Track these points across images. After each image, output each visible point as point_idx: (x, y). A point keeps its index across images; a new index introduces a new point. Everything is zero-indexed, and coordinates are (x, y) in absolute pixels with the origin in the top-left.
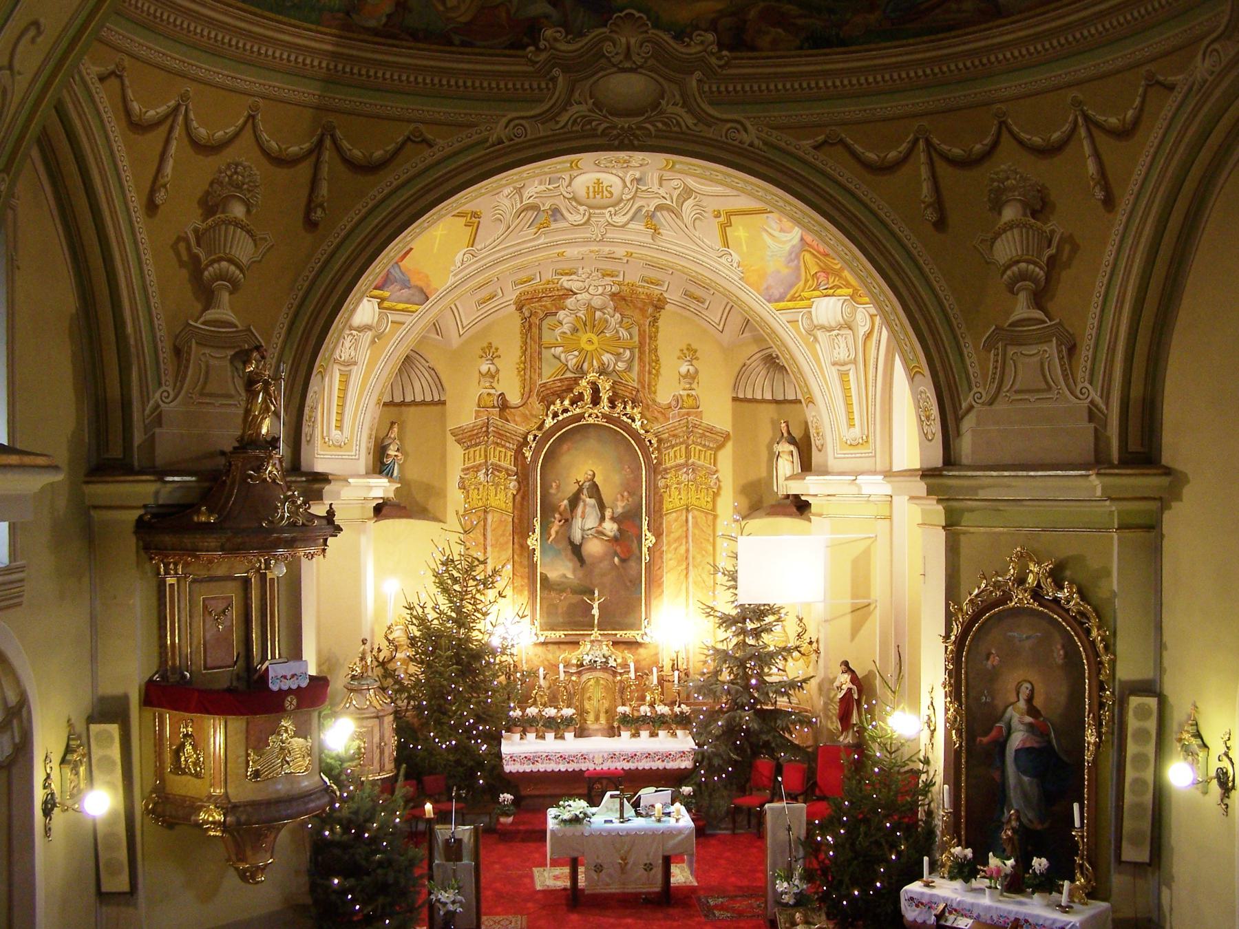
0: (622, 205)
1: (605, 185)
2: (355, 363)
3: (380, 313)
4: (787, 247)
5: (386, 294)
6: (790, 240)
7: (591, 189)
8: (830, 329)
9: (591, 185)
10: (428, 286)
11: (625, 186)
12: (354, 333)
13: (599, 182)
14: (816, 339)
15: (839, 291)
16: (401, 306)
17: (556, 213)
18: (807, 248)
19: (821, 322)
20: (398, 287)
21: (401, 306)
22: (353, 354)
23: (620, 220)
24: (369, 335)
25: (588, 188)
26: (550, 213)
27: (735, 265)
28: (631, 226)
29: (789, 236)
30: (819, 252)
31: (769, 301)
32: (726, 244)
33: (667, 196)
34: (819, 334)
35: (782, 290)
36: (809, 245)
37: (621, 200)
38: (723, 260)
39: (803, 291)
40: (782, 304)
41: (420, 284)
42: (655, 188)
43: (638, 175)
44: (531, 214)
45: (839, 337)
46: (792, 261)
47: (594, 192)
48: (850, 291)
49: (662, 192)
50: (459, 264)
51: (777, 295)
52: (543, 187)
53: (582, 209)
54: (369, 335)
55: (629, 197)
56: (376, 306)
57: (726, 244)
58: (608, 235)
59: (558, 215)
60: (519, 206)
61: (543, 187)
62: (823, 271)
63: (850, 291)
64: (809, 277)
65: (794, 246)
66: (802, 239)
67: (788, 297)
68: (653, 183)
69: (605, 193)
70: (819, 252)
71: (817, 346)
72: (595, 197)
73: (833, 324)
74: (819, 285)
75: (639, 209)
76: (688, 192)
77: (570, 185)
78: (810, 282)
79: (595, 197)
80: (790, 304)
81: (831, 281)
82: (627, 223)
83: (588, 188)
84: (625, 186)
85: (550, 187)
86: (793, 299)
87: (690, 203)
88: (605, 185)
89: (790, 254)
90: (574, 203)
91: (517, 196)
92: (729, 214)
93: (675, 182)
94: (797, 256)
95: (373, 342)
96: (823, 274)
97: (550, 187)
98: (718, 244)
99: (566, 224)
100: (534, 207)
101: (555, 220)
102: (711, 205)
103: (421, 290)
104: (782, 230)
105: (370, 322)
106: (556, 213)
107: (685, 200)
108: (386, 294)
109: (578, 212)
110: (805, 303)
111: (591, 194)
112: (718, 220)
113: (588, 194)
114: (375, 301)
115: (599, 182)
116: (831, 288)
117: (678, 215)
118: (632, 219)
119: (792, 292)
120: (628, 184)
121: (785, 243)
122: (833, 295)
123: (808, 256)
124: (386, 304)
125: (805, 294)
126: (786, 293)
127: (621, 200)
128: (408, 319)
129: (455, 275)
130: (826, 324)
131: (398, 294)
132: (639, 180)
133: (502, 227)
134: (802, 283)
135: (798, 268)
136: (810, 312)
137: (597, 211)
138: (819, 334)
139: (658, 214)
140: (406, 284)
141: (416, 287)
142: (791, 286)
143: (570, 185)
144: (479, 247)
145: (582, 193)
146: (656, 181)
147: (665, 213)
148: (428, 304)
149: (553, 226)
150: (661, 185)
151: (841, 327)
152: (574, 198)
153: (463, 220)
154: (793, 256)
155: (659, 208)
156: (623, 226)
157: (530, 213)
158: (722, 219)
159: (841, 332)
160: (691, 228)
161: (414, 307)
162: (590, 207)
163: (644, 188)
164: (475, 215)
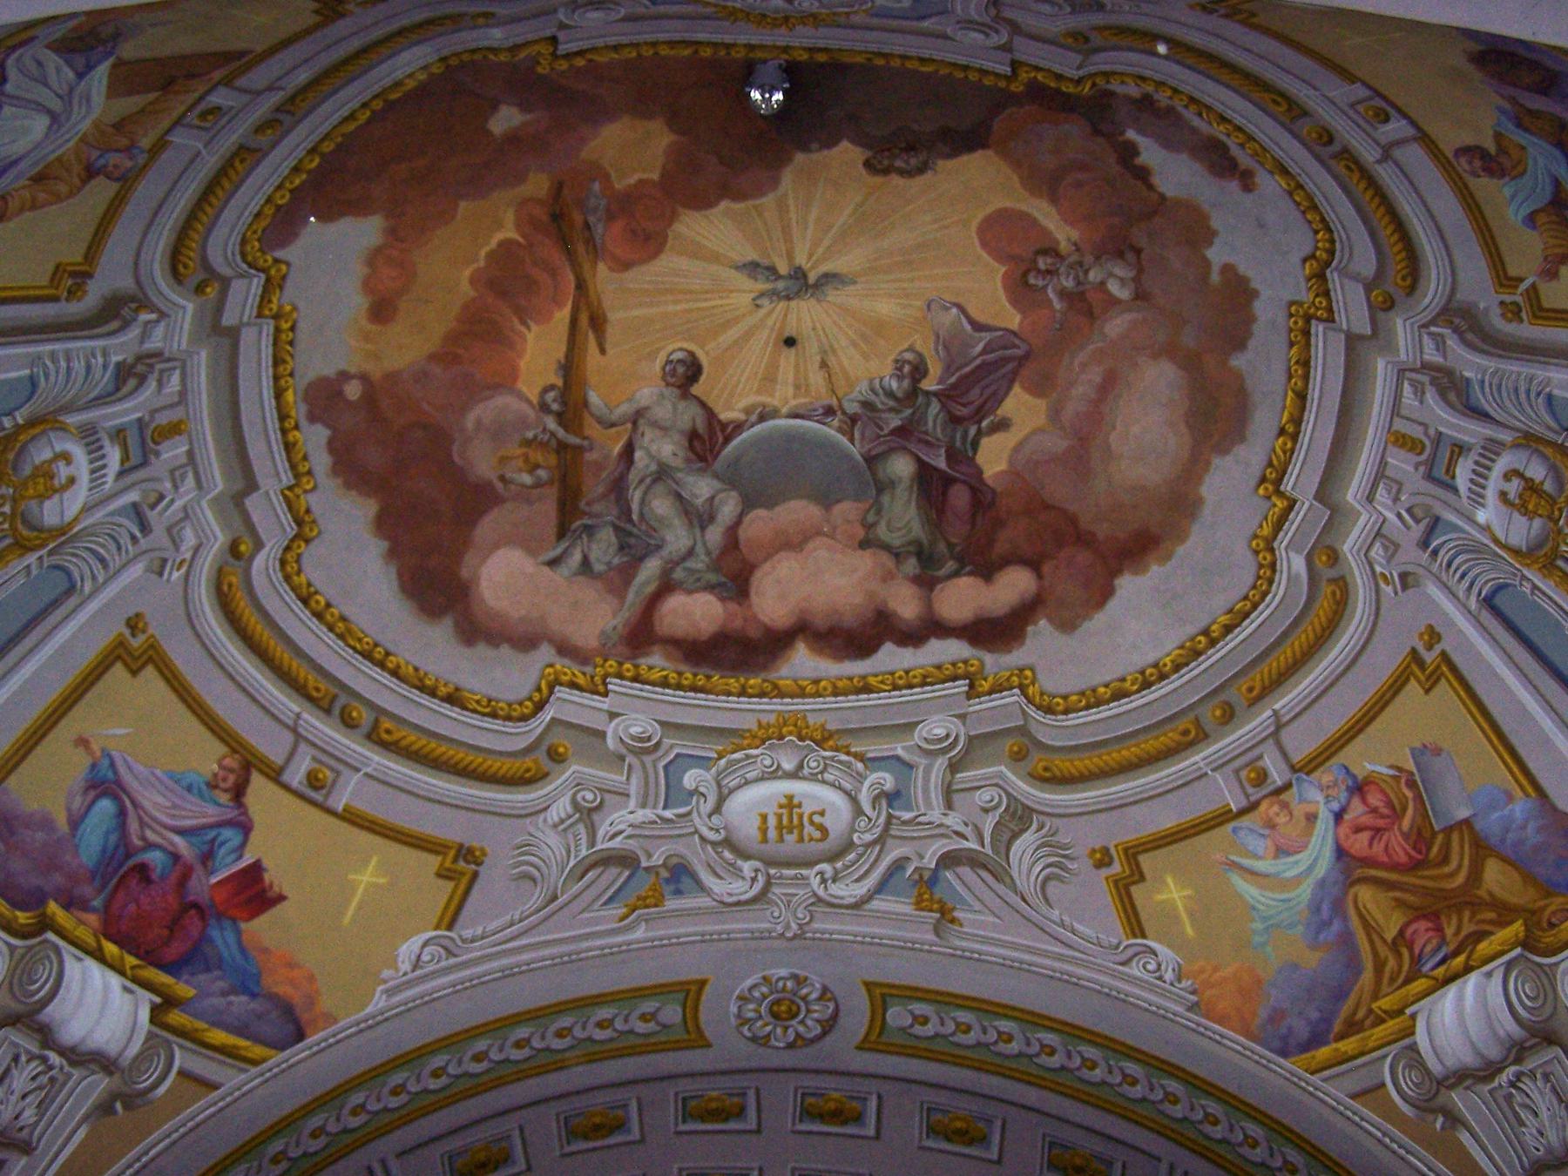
0: (852, 856)
1: (807, 809)
2: (26, 1148)
3: (151, 1036)
4: (1305, 892)
5: (184, 990)
6: (1311, 868)
7: (772, 821)
8: (1489, 1071)
9: (771, 811)
10: (311, 1001)
11: (858, 812)
12: (54, 1058)
13: (790, 803)
14: (1454, 1120)
15: (1484, 947)
16: (219, 1037)
17: (679, 875)
18: (1359, 872)
19: (1451, 1063)
20: (221, 984)
21: (219, 1037)
22: (29, 1115)
23: (847, 891)
24: (100, 1084)
25: (764, 818)
26: (665, 874)
27: (1169, 976)
28: (876, 904)
29: (1304, 859)
30: (1395, 867)
31: (1284, 1053)
32: (1135, 926)
33: (968, 831)
34: (1457, 1099)
35: (1314, 1015)
36: (1367, 862)
37: (849, 846)
38: (1135, 970)
39: (1376, 996)
40: (1324, 1053)
41: (282, 989)
42: (935, 815)
43: (888, 781)
44: (614, 876)
45: (1526, 1085)
46: (1326, 924)
47: (780, 827)
48: (1517, 928)
49: (953, 820)
50: (406, 966)
51: (1302, 1031)
52: (645, 814)
53: (747, 867)
54: (100, 1084)
55: (868, 837)
56: (144, 1014)
57: (1135, 926)
58: (815, 925)
59: (686, 882)
60: (584, 852)
61: (645, 814)
62: (1420, 914)
63: (1517, 928)
64: (1383, 951)
65: (1321, 884)
66: (1341, 852)
67: (1337, 1026)
68: (929, 805)
69: (808, 829)
70: (1395, 867)
71: (1465, 1137)
72: (781, 839)
73: (1494, 1053)
74: (1417, 961)
75: (899, 865)
76: (1018, 817)
77: (717, 810)
78: (1391, 963)
79: (781, 839)
80: (1348, 1045)
81: (1449, 931)
82: (869, 898)
83: (764, 818)
84: (858, 812)
85: (668, 814)
86: (1353, 1027)
87: (1025, 843)
88: (807, 809)
89: (1315, 907)
90: (727, 854)
91: (581, 828)
92: (1132, 853)
93: (983, 796)
94: (1338, 906)
95: (105, 1108)
96: (1422, 925)
97: (668, 814)
98: (1112, 928)
99: (703, 901)
100: (626, 860)
101: (678, 892)
102: (1084, 837)
103: (287, 1010)
104: (1281, 851)
105: (112, 1049)
106: (679, 875)
107: (1015, 836)
108: (184, 990)
109: (737, 873)
110: (1392, 1025)
111: (772, 834)
112: (1105, 872)
113: (764, 831)
114: (146, 999)
115: (790, 803)
116: (1456, 953)
117: (1000, 874)
118: (880, 888)
119: (1350, 1002)
120: (867, 808)
121: (1297, 880)
122: (1468, 969)
123: (1365, 894)
124: (176, 1017)
125: (1385, 1003)
126: (1328, 1021)
127: (849, 846)
128: (232, 1079)
129: (390, 992)
130: (1469, 1059)
131: (218, 1001)
132: (892, 797)
133: (537, 896)
134: (1368, 976)
135: (1346, 939)
136: (1413, 1048)
137: (787, 872)
138: (1457, 1099)
139: (948, 874)
140: (247, 984)
141: (273, 998)
142: (1340, 995)
143: (717, 810)
144: (468, 933)
145: (748, 830)
146: (936, 798)
147: (965, 871)
148: (299, 1052)
149: (672, 904)
150: (949, 805)
151: (1518, 1051)
152: (728, 843)
153: (434, 861)
154: (1325, 907)
155: (949, 860)
156: (858, 905)
157: (613, 871)
158: (1116, 868)
159: (1529, 1064)
160: (1038, 901)
161: (258, 1051)
162: (770, 863)
163: (907, 816)
164: (467, 854)
